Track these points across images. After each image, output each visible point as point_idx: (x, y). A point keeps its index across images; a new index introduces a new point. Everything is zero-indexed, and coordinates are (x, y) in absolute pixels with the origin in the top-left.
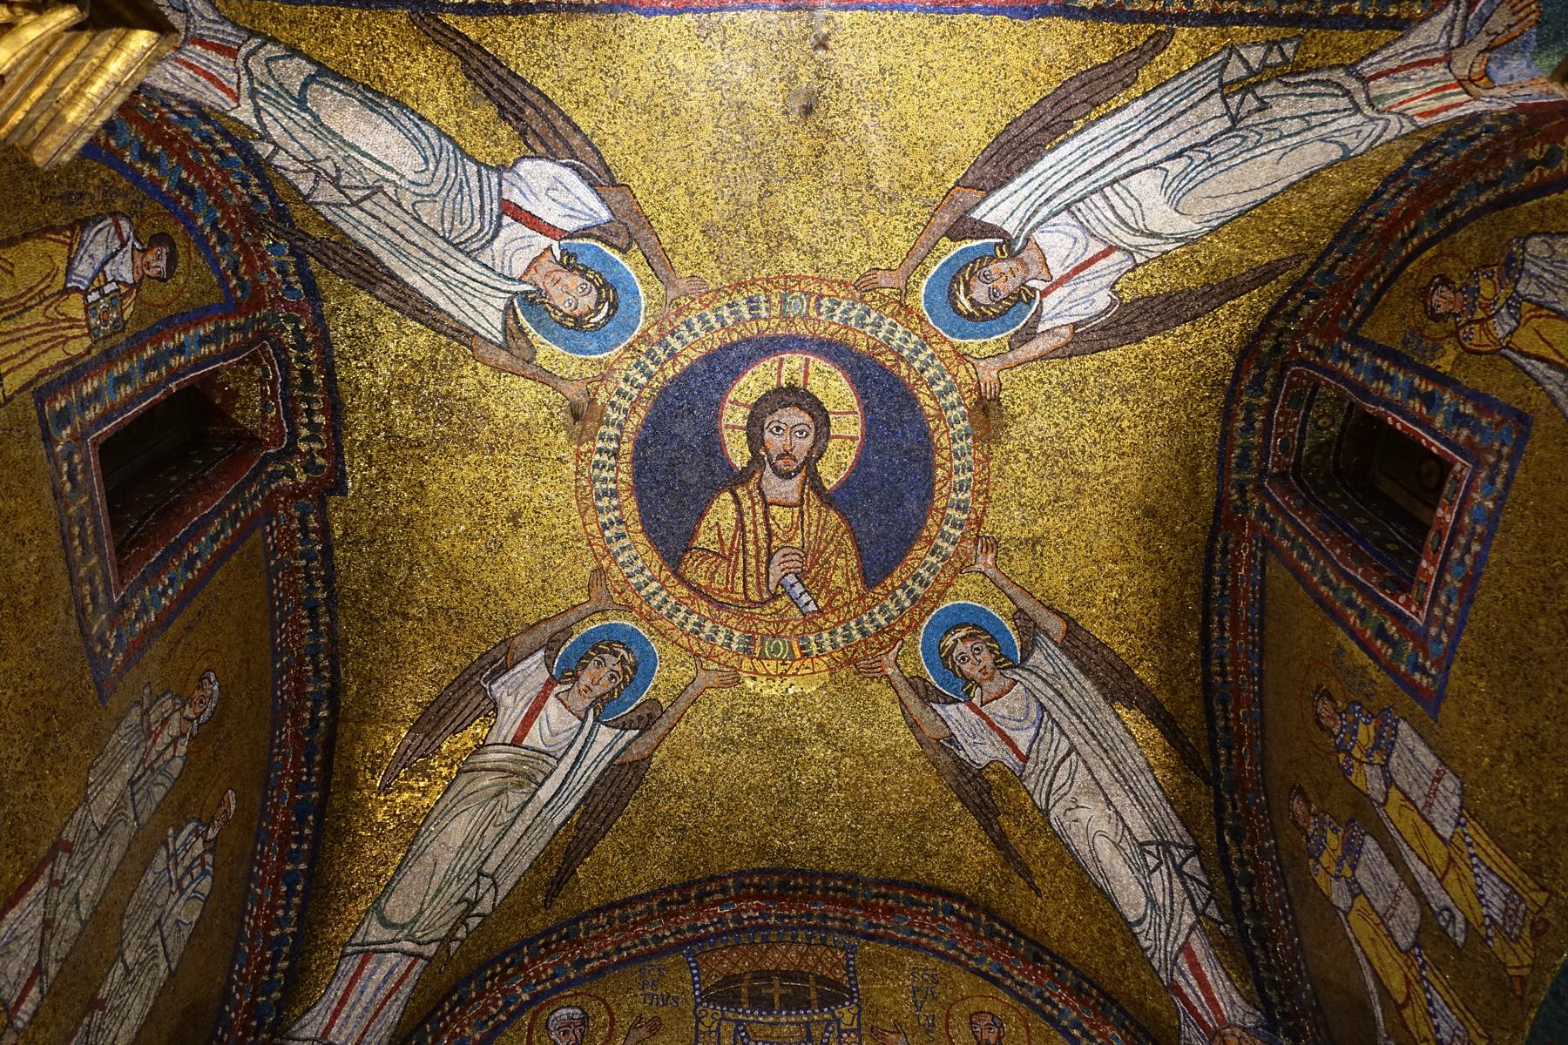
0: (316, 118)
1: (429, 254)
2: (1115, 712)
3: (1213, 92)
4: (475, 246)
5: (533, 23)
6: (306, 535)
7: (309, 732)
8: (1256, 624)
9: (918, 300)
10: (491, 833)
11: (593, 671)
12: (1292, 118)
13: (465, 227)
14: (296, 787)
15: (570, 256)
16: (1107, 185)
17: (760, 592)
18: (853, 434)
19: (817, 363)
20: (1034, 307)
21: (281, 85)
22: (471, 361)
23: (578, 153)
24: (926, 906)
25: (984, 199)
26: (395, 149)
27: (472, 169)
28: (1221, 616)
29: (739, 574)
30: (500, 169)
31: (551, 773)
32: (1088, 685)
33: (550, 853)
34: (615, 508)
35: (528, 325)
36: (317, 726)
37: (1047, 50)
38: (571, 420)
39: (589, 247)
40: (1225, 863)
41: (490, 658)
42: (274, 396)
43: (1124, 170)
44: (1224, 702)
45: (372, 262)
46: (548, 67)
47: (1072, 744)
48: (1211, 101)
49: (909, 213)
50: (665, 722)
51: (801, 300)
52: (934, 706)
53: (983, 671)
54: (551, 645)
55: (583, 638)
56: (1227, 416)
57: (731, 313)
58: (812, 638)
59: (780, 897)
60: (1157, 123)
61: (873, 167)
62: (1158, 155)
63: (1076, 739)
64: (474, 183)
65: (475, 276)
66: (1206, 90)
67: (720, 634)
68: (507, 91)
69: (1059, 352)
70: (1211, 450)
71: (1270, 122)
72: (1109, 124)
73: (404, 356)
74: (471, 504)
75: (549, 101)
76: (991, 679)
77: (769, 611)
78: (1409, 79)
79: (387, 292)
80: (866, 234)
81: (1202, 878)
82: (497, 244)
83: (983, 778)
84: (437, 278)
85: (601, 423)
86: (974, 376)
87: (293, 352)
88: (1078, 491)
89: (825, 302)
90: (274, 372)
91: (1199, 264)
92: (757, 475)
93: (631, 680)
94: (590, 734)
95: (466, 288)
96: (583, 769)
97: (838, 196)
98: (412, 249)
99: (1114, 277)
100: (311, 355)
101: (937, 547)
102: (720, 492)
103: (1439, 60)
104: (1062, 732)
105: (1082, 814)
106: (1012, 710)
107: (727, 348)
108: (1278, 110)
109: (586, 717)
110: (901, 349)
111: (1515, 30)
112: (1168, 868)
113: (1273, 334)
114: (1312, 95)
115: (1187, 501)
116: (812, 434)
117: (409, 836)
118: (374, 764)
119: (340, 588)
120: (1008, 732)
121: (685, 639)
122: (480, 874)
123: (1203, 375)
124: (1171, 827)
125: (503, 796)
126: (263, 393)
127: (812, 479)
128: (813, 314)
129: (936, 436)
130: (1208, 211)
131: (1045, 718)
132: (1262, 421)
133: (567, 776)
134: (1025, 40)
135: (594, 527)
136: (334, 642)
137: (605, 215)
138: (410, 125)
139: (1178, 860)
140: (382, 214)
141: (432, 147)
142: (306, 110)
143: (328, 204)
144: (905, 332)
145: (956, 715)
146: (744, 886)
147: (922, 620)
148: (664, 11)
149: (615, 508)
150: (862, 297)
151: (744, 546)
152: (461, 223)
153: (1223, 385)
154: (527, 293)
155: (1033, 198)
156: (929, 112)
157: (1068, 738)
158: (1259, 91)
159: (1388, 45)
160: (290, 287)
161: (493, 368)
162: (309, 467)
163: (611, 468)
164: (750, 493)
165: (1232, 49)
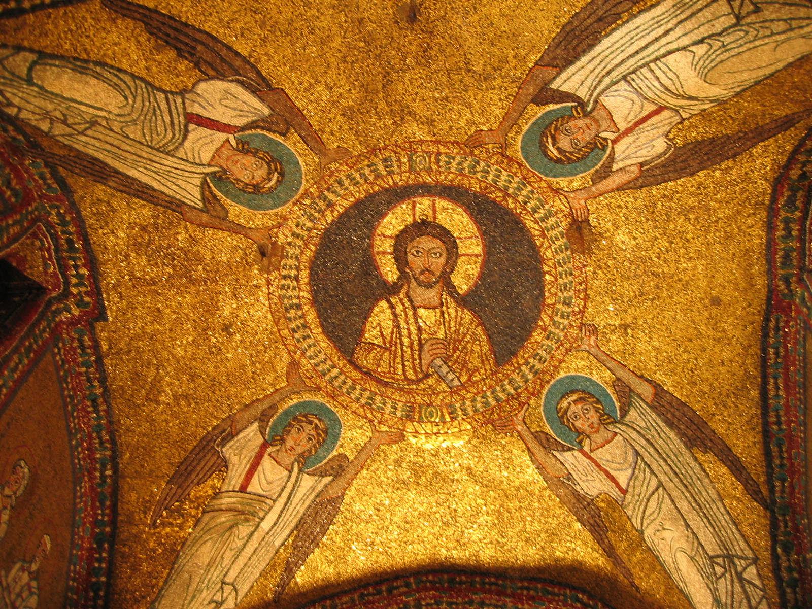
0: (41, 88)
1: (140, 157)
2: (693, 455)
4: (171, 148)
6: (83, 350)
7: (100, 485)
8: (802, 386)
9: (517, 149)
10: (229, 556)
11: (295, 435)
12: (779, 20)
13: (161, 137)
14: (96, 523)
15: (243, 143)
16: (651, 62)
17: (415, 372)
18: (476, 252)
19: (441, 203)
20: (608, 152)
22: (183, 223)
24: (558, 595)
25: (558, 74)
26: (102, 95)
27: (161, 96)
28: (776, 378)
29: (399, 360)
30: (183, 93)
31: (270, 510)
32: (672, 435)
33: (274, 565)
34: (300, 317)
35: (219, 194)
36: (105, 481)
38: (260, 256)
39: (257, 136)
40: (776, 569)
41: (221, 429)
42: (50, 259)
43: (663, 51)
44: (779, 446)
45: (102, 165)
47: (659, 481)
49: (501, 88)
50: (351, 471)
51: (424, 158)
52: (555, 453)
53: (591, 426)
54: (263, 418)
55: (286, 413)
56: (770, 227)
57: (371, 171)
58: (458, 405)
59: (450, 589)
60: (683, 16)
61: (469, 56)
62: (686, 41)
63: (663, 477)
64: (163, 105)
65: (175, 166)
67: (389, 406)
69: (631, 185)
70: (760, 253)
71: (763, 22)
73: (135, 223)
74: (195, 321)
76: (597, 431)
77: (422, 386)
79: (116, 182)
80: (470, 105)
81: (757, 582)
82: (187, 144)
83: (594, 505)
84: (149, 170)
85: (282, 257)
86: (567, 205)
87: (59, 229)
88: (657, 287)
89: (443, 158)
90: (48, 242)
91: (732, 118)
92: (405, 287)
93: (324, 441)
94: (297, 481)
95: (171, 174)
96: (293, 505)
97: (444, 79)
98: (127, 155)
99: (667, 128)
100: (72, 229)
101: (551, 332)
102: (377, 300)
104: (652, 472)
105: (666, 534)
106: (613, 456)
107: (371, 197)
109: (292, 468)
110: (507, 188)
112: (731, 575)
113: (800, 166)
115: (745, 290)
116: (444, 255)
117: (172, 558)
118: (145, 507)
119: (111, 385)
120: (611, 472)
121: (361, 410)
122: (223, 583)
123: (747, 198)
124: (735, 543)
125: (235, 530)
126: (43, 256)
127: (448, 288)
128: (434, 167)
129: (542, 250)
131: (639, 461)
132: (798, 230)
133: (282, 512)
135: (286, 332)
136: (110, 422)
137: (267, 111)
139: (739, 569)
140: (101, 136)
144: (509, 176)
145: (571, 459)
146: (423, 582)
147: (542, 387)
149: (300, 317)
150: (472, 153)
151: (400, 339)
152: (158, 135)
153: (763, 204)
154: (215, 173)
155: (597, 71)
156: (508, 12)
157: (657, 477)
160: (49, 186)
161: (199, 226)
162: (80, 303)
163: (294, 288)
164: (401, 300)
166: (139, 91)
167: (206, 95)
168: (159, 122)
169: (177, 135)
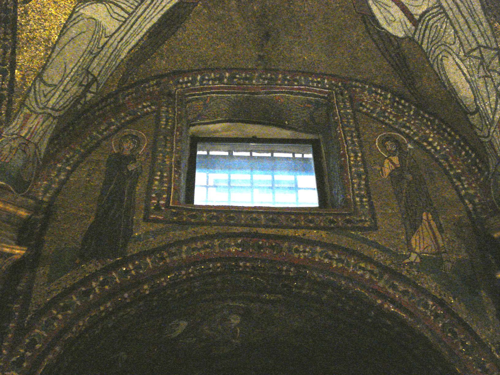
0: (475, 100)
4: (435, 10)
12: (71, 88)
13: (436, 24)
16: (128, 18)
23: (376, 31)
26: (452, 71)
27: (424, 46)
43: (122, 28)
48: (98, 73)
62: (111, 41)
64: (425, 41)
72: (133, 43)
82: (425, 8)
108: (76, 87)
114: (68, 100)
130: (81, 23)
138: (443, 76)
140: (471, 38)
141: (437, 64)
142: (477, 105)
143: (491, 49)
148: (326, 75)
158: (83, 88)
166: (433, 58)
167: (401, 28)
168: (432, 34)
169: (428, 18)
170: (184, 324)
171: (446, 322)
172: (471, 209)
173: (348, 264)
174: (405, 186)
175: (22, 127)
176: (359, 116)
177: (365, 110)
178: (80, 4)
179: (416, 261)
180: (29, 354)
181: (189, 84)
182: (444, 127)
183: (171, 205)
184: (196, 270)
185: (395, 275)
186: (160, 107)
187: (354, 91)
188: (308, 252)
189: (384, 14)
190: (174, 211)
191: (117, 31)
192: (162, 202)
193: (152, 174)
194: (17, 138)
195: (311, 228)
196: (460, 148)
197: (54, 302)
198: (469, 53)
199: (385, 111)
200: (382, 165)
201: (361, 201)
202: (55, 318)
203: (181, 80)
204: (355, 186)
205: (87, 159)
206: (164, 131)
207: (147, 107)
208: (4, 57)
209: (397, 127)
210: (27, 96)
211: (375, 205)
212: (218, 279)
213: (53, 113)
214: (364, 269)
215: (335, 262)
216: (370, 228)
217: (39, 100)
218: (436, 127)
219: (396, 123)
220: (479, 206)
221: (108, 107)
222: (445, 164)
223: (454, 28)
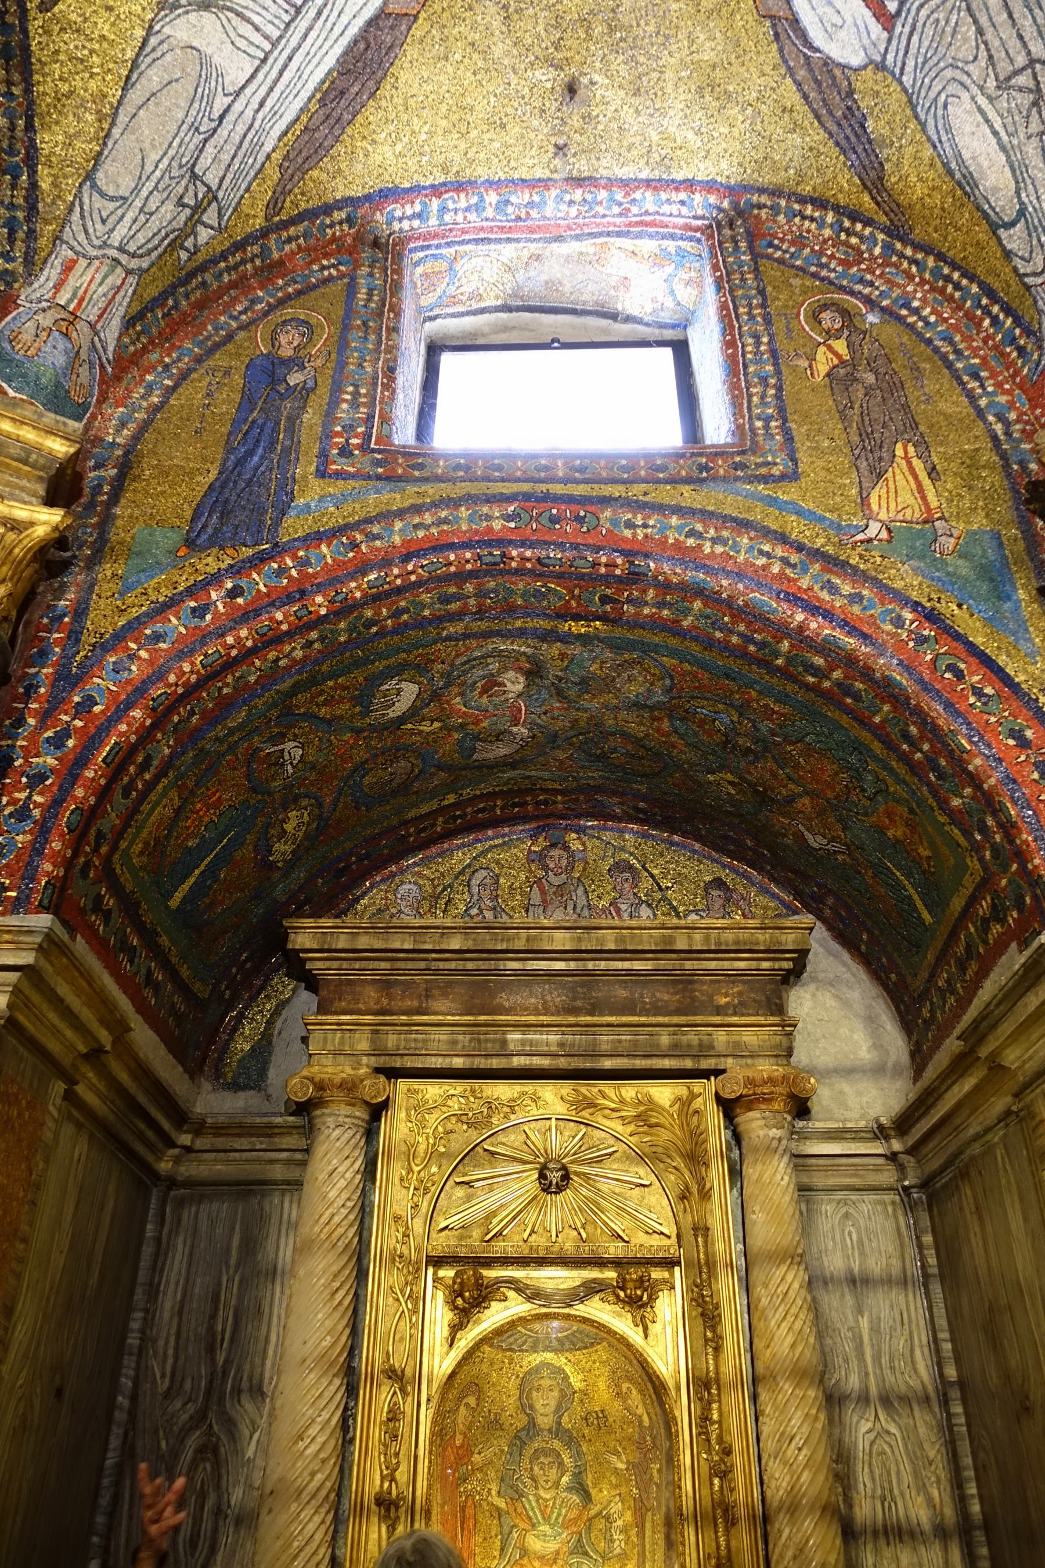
0: (1018, 192)
3: (219, 188)
5: (814, 189)
13: (935, 15)
16: (271, 52)
21: (1030, 235)
26: (968, 128)
30: (881, 67)
37: (360, 166)
43: (260, 76)
46: (811, 149)
48: (217, 180)
60: (250, 136)
61: (504, 29)
62: (238, 107)
66: (224, 187)
68: (853, 139)
72: (289, 117)
75: (817, 117)
78: (104, 295)
103: (97, 322)
108: (169, 206)
111: (74, 377)
114: (155, 235)
130: (168, 57)
134: (381, 171)
138: (946, 145)
140: (1014, 44)
142: (1021, 203)
152: (937, 20)
155: (335, 13)
158: (188, 211)
159: (129, 306)
165: (220, 230)
168: (926, 43)
170: (409, 691)
171: (942, 651)
172: (999, 433)
173: (736, 547)
174: (860, 394)
175: (58, 287)
176: (764, 264)
177: (779, 254)
178: (163, 13)
179: (880, 537)
180: (79, 723)
181: (416, 223)
182: (946, 271)
183: (372, 446)
184: (422, 567)
185: (834, 563)
186: (357, 266)
187: (757, 217)
188: (653, 527)
189: (820, 11)
190: (379, 456)
191: (249, 81)
192: (355, 441)
193: (337, 388)
194: (49, 308)
195: (659, 481)
196: (979, 312)
197: (133, 627)
198: (1008, 79)
199: (821, 253)
200: (812, 359)
201: (767, 427)
202: (133, 657)
203: (398, 213)
204: (755, 399)
205: (205, 365)
206: (364, 310)
207: (329, 267)
208: (12, 137)
209: (845, 283)
210: (65, 221)
211: (794, 433)
212: (469, 587)
213: (124, 259)
214: (768, 555)
215: (708, 544)
216: (783, 477)
217: (91, 231)
218: (927, 276)
219: (843, 275)
220: (1018, 427)
221: (249, 266)
222: (946, 348)
223: (976, 22)
